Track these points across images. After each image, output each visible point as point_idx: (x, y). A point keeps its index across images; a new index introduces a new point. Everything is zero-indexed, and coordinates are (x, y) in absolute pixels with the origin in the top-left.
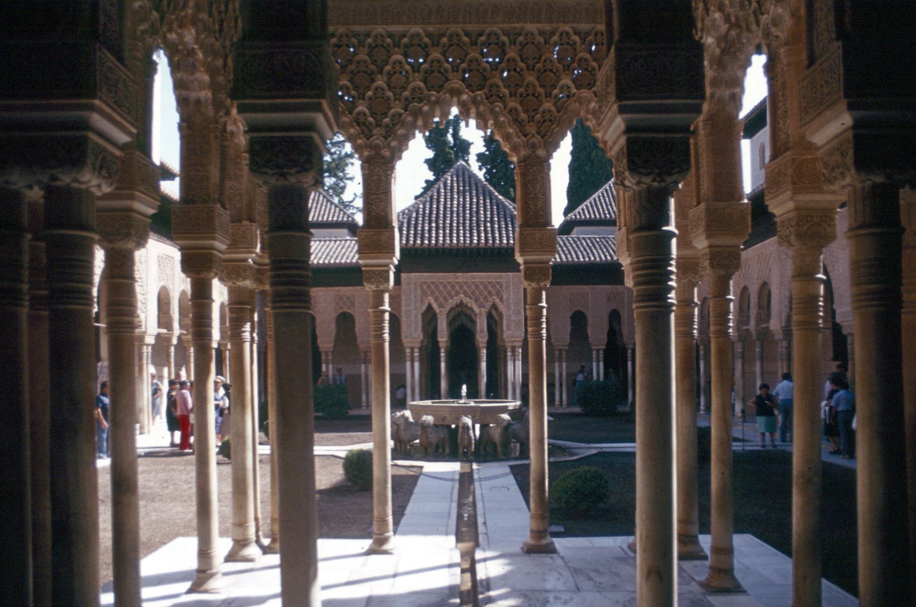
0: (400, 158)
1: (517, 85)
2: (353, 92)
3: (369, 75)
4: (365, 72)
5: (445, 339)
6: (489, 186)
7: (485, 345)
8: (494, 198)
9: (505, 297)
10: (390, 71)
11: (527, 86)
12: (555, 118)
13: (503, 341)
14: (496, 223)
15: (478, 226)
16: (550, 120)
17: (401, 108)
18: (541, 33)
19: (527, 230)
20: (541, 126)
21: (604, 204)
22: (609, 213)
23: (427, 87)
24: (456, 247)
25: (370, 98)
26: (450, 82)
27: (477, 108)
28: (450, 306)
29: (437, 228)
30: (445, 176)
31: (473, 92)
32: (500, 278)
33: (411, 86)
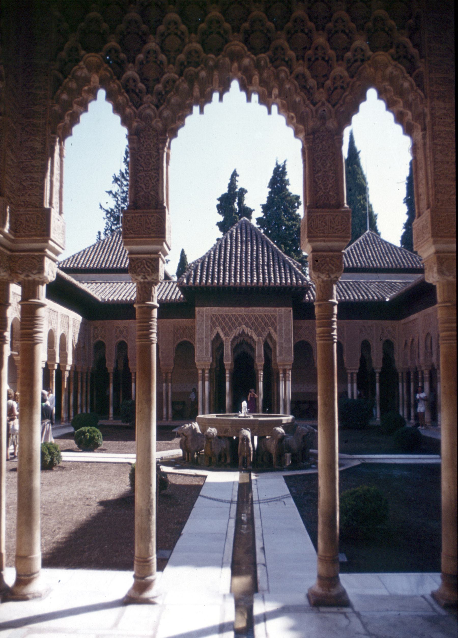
1: (305, 48)
5: (230, 363)
6: (266, 237)
8: (270, 246)
10: (164, 33)
11: (316, 49)
12: (348, 84)
13: (276, 364)
14: (272, 266)
15: (258, 269)
21: (355, 255)
22: (360, 262)
24: (239, 286)
25: (141, 63)
27: (261, 75)
28: (234, 335)
29: (225, 270)
30: (232, 229)
32: (275, 311)
33: (186, 48)
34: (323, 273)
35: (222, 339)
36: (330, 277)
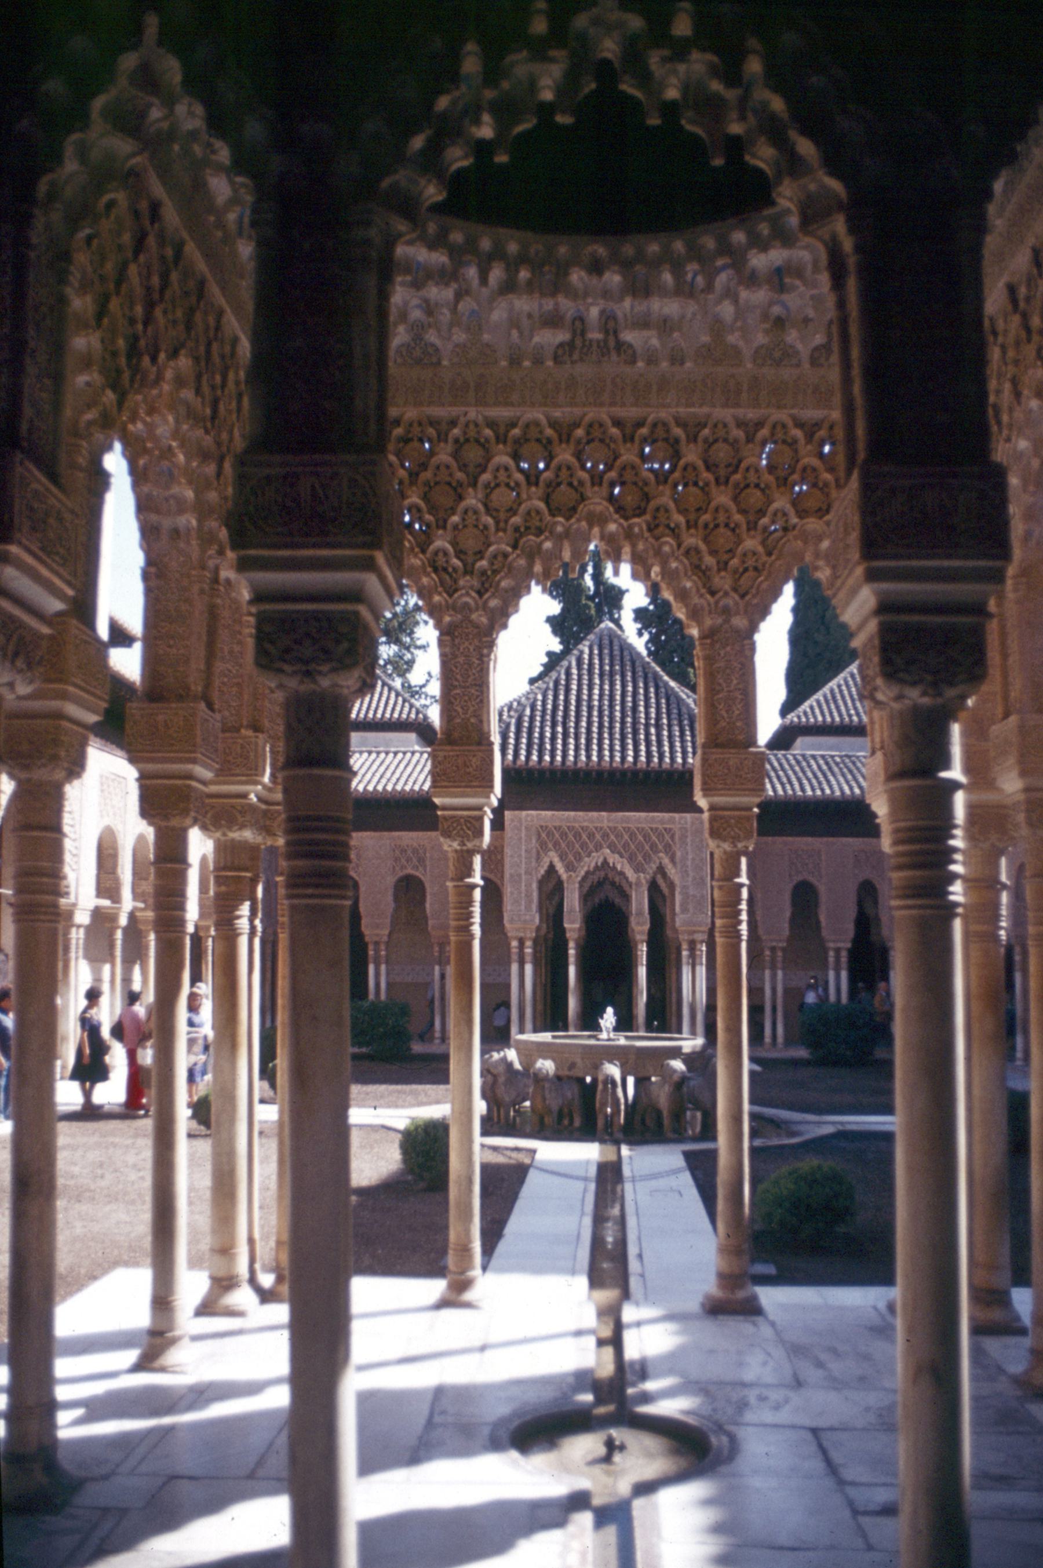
0: (504, 626)
1: (698, 510)
2: (428, 517)
3: (455, 489)
4: (449, 484)
5: (577, 926)
6: (653, 665)
7: (645, 937)
8: (661, 684)
9: (679, 854)
10: (489, 483)
11: (717, 510)
12: (764, 565)
14: (665, 727)
15: (635, 732)
16: (756, 569)
17: (508, 545)
18: (740, 424)
19: (713, 753)
20: (740, 578)
21: (848, 698)
22: (858, 714)
23: (550, 510)
24: (596, 767)
25: (455, 527)
26: (586, 502)
27: (634, 546)
28: (586, 869)
29: (566, 735)
30: (580, 647)
31: (626, 519)
32: (672, 821)
33: (523, 508)
34: (725, 841)
35: (559, 877)
36: (735, 846)
